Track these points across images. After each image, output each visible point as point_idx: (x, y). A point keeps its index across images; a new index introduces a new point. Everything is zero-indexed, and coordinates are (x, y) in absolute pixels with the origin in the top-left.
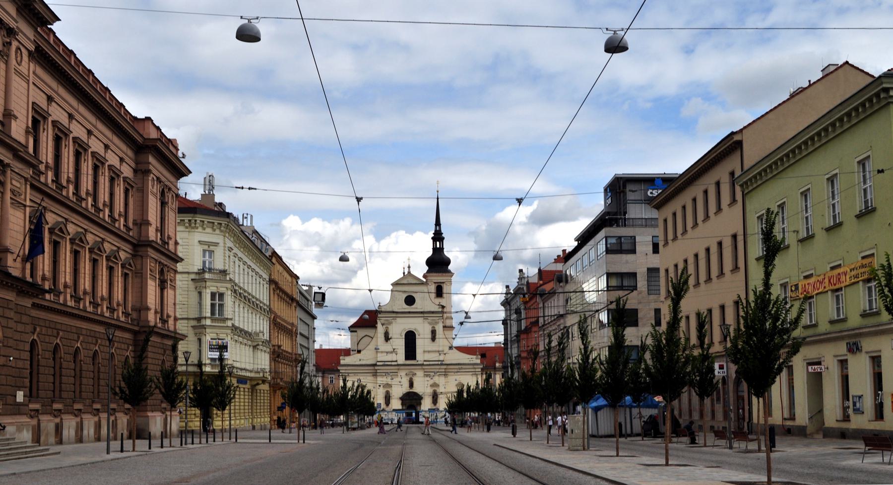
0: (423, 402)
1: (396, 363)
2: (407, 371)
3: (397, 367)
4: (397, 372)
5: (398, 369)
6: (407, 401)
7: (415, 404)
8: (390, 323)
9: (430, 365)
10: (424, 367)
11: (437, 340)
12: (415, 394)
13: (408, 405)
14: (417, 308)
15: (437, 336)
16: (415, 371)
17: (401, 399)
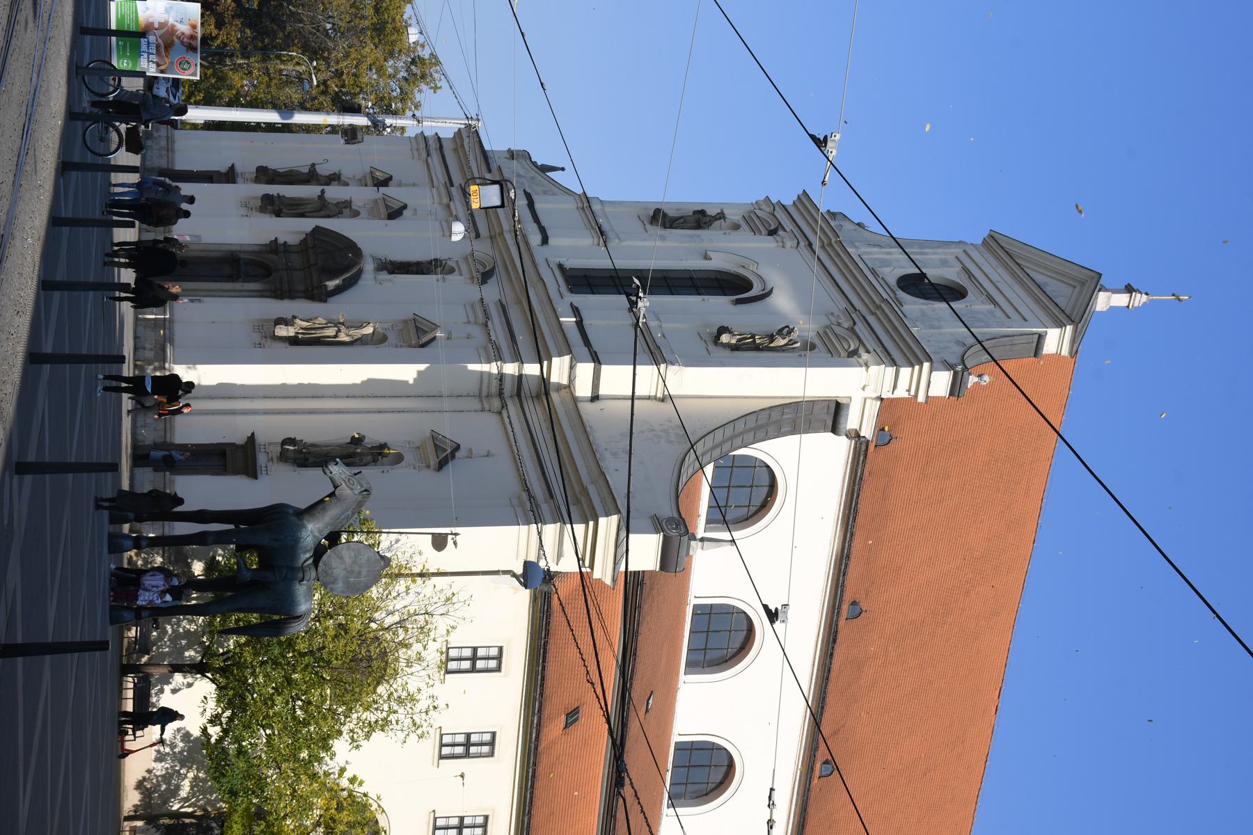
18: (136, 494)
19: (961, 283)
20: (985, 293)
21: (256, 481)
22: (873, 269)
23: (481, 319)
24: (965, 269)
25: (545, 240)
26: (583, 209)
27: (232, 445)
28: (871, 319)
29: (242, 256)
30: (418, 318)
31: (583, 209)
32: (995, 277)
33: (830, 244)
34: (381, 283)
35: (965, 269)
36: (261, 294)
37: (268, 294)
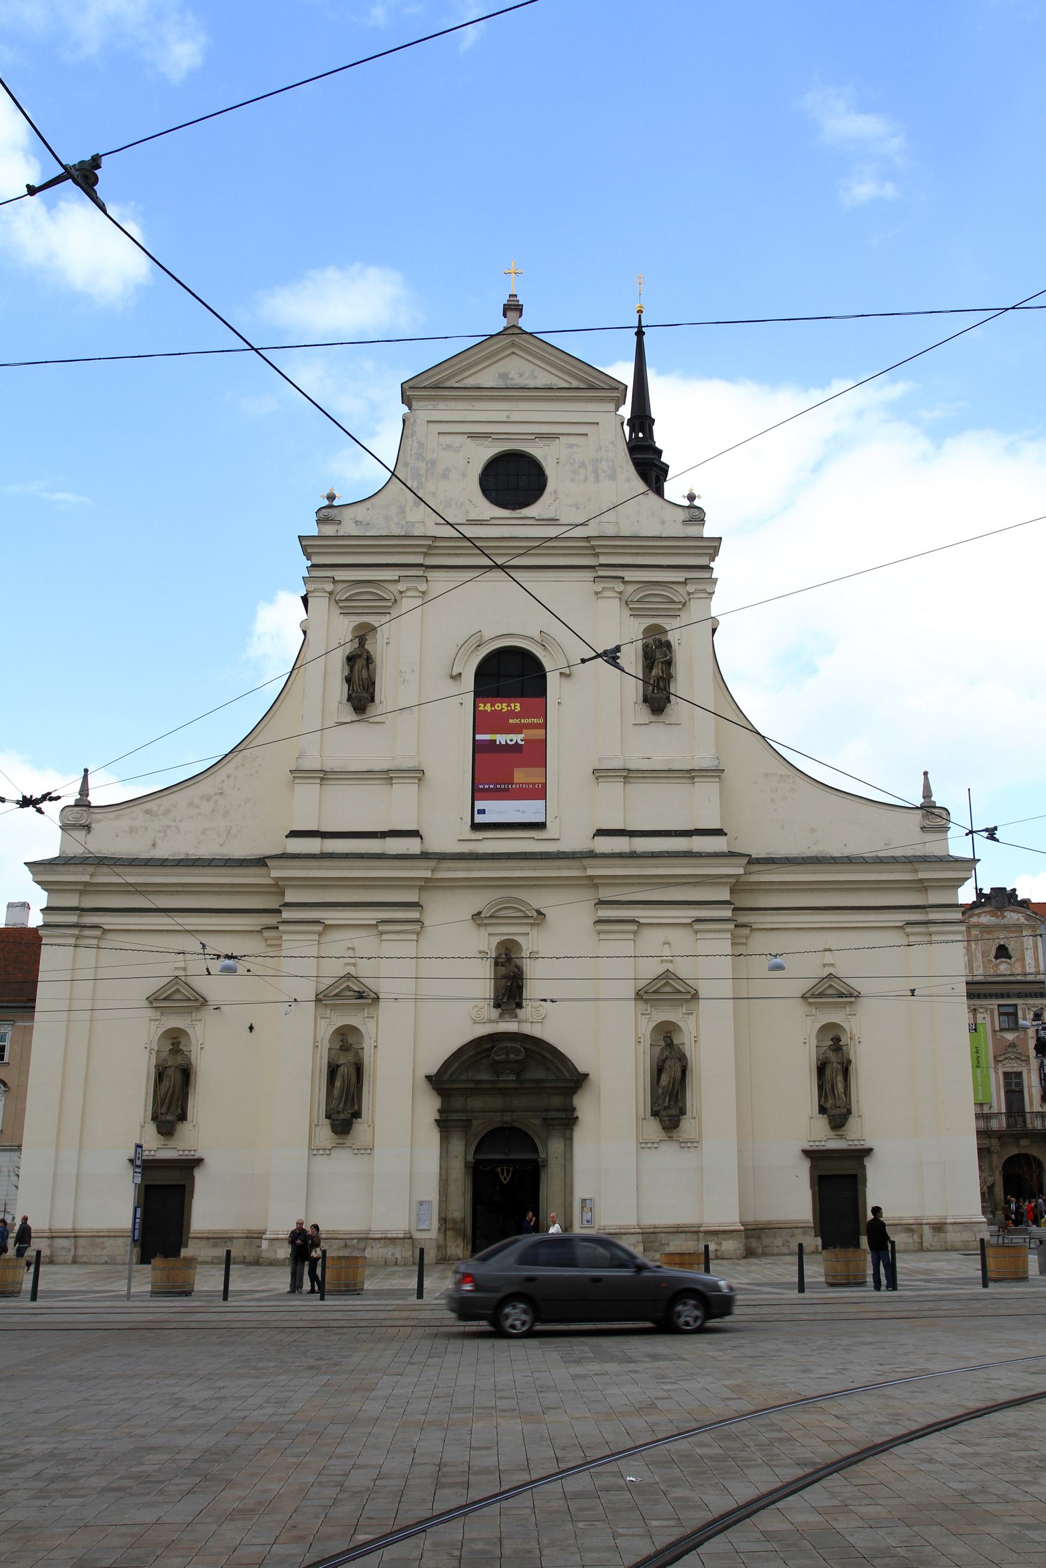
0: (584, 1104)
1: (411, 846)
4: (416, 905)
5: (426, 885)
6: (477, 1103)
7: (532, 1124)
8: (386, 606)
9: (633, 855)
10: (596, 870)
11: (677, 709)
13: (480, 1126)
14: (553, 521)
16: (537, 900)
17: (439, 1082)
18: (181, 1248)
20: (533, 437)
22: (467, 520)
23: (634, 927)
24: (473, 436)
25: (414, 834)
28: (603, 560)
29: (470, 1158)
30: (645, 989)
32: (502, 416)
33: (430, 547)
34: (542, 1019)
35: (473, 436)
36: (569, 1140)
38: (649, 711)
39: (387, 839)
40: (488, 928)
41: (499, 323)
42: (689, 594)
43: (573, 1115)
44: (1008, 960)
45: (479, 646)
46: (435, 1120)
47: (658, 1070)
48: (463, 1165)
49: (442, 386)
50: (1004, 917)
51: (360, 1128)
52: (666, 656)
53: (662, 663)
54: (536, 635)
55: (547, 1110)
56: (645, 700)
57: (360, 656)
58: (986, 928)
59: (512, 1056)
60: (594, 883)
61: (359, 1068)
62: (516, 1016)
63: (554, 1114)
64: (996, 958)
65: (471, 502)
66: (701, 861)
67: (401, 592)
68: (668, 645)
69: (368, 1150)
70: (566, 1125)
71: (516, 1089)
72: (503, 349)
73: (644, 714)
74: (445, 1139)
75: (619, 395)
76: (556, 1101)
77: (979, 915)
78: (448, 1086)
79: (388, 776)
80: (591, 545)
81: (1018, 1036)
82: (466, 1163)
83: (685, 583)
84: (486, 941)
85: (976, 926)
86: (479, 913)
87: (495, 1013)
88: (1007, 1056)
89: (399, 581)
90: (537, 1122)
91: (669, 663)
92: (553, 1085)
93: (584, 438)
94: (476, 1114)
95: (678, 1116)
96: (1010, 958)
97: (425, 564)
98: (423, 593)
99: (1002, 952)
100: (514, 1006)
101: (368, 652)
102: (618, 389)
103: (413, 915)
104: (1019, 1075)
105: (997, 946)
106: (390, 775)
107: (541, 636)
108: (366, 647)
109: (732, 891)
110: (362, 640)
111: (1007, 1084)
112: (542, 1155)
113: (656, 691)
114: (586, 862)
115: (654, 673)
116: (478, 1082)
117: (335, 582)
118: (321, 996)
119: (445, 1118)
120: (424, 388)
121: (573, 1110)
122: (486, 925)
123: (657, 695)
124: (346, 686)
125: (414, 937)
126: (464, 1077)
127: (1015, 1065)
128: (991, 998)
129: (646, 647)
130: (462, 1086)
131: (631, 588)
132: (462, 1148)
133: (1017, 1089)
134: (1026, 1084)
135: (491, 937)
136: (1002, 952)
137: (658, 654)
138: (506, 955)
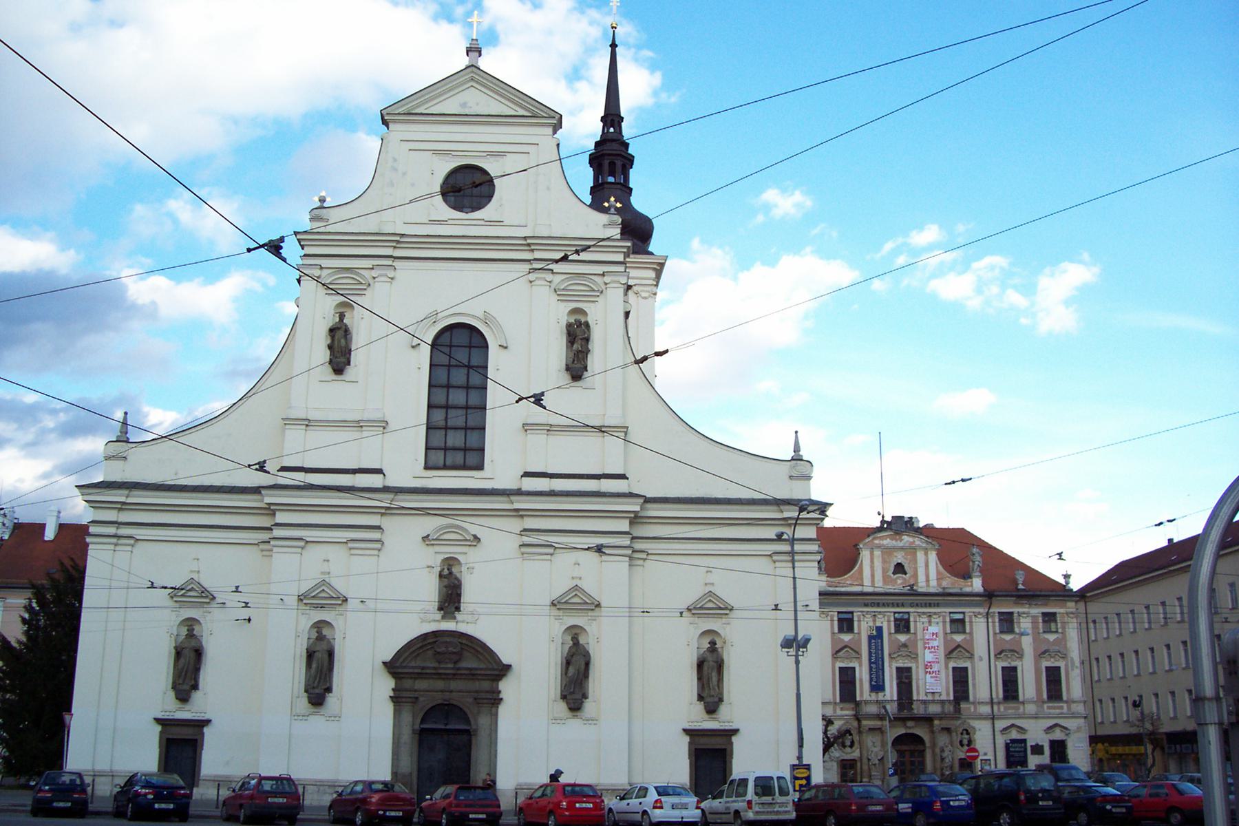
1: (374, 481)
2: (430, 524)
3: (384, 500)
4: (379, 528)
5: (387, 511)
6: (421, 684)
7: (465, 702)
8: (363, 287)
9: (552, 493)
12: (471, 645)
13: (426, 702)
15: (595, 361)
16: (473, 526)
19: (460, 164)
20: (485, 154)
21: (741, 730)
24: (436, 152)
25: (379, 471)
26: (307, 425)
27: (690, 743)
28: (538, 255)
29: (417, 727)
31: (307, 425)
33: (398, 242)
35: (436, 152)
37: (494, 710)
38: (570, 377)
39: (357, 475)
40: (435, 547)
41: (463, 61)
42: (606, 284)
43: (498, 696)
44: (904, 576)
45: (435, 322)
46: (391, 697)
47: (568, 663)
48: (411, 732)
49: (413, 112)
50: (901, 540)
51: (331, 699)
52: (584, 334)
53: (581, 339)
54: (480, 314)
55: (477, 692)
56: (568, 369)
57: (339, 329)
58: (888, 551)
59: (450, 649)
60: (518, 513)
61: (331, 654)
62: (455, 618)
63: (483, 695)
64: (894, 573)
65: (433, 206)
66: (604, 500)
67: (374, 278)
68: (587, 325)
69: (337, 717)
70: (493, 704)
71: (454, 675)
72: (464, 83)
73: (565, 378)
74: (397, 713)
75: (556, 122)
76: (486, 685)
77: (881, 538)
78: (400, 670)
79: (359, 425)
80: (528, 243)
81: (909, 639)
82: (413, 730)
83: (603, 275)
84: (434, 557)
85: (879, 547)
86: (428, 535)
87: (439, 616)
88: (900, 654)
89: (372, 269)
90: (471, 700)
91: (587, 340)
92: (483, 672)
93: (527, 155)
94: (422, 693)
95: (581, 700)
96: (906, 573)
97: (394, 255)
98: (392, 279)
99: (899, 568)
100: (454, 609)
101: (346, 326)
102: (554, 117)
103: (375, 535)
104: (909, 670)
105: (895, 564)
106: (361, 424)
107: (485, 315)
108: (344, 321)
109: (631, 523)
110: (342, 316)
111: (899, 678)
112: (474, 727)
113: (576, 362)
114: (513, 498)
115: (575, 346)
116: (423, 668)
117: (321, 268)
118: (302, 597)
119: (397, 695)
120: (399, 114)
121: (499, 692)
122: (433, 545)
123: (576, 366)
124: (328, 352)
125: (376, 552)
126: (413, 664)
127: (906, 661)
128: (888, 606)
129: (569, 326)
130: (411, 671)
131: (557, 279)
132: (410, 719)
133: (907, 681)
134: (914, 677)
135: (438, 555)
136: (899, 568)
137: (578, 332)
138: (448, 569)
